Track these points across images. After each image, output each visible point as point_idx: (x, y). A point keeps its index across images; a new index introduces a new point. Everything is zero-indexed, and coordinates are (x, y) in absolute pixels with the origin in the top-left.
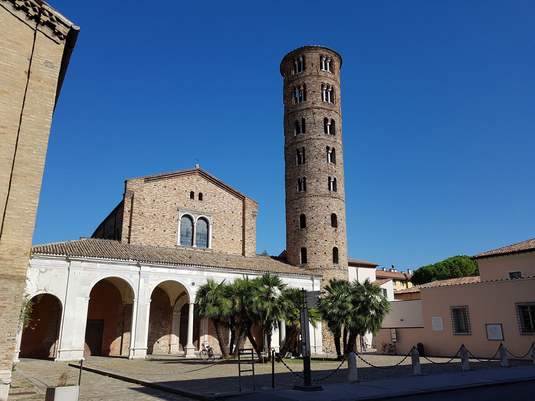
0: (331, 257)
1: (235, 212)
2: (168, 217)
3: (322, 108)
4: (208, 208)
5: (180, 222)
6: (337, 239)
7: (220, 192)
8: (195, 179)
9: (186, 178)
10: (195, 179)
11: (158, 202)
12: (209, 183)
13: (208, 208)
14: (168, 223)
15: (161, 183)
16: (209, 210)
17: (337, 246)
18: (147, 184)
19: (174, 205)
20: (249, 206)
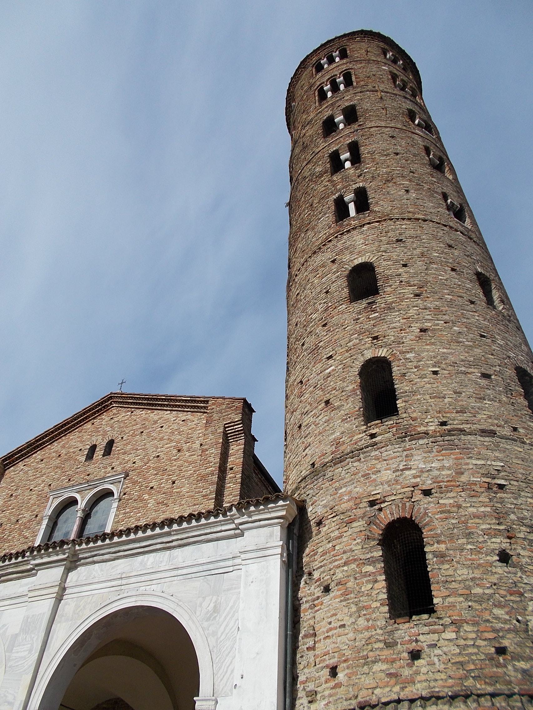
0: (354, 404)
1: (185, 447)
2: (24, 520)
3: (317, 115)
4: (121, 464)
5: (45, 522)
6: (380, 330)
7: (156, 418)
8: (107, 419)
9: (88, 426)
10: (107, 419)
11: (16, 496)
12: (138, 412)
13: (121, 464)
14: (20, 535)
15: (38, 455)
16: (119, 469)
17: (382, 353)
18: (12, 468)
19: (47, 489)
20: (216, 417)
